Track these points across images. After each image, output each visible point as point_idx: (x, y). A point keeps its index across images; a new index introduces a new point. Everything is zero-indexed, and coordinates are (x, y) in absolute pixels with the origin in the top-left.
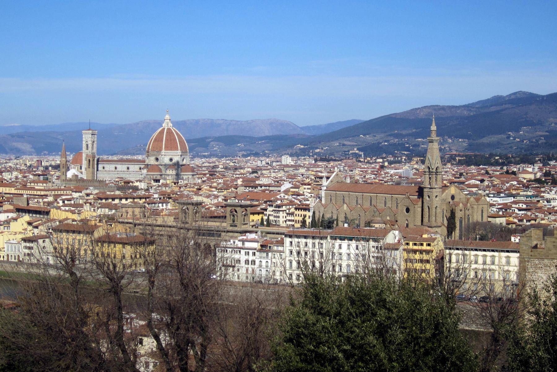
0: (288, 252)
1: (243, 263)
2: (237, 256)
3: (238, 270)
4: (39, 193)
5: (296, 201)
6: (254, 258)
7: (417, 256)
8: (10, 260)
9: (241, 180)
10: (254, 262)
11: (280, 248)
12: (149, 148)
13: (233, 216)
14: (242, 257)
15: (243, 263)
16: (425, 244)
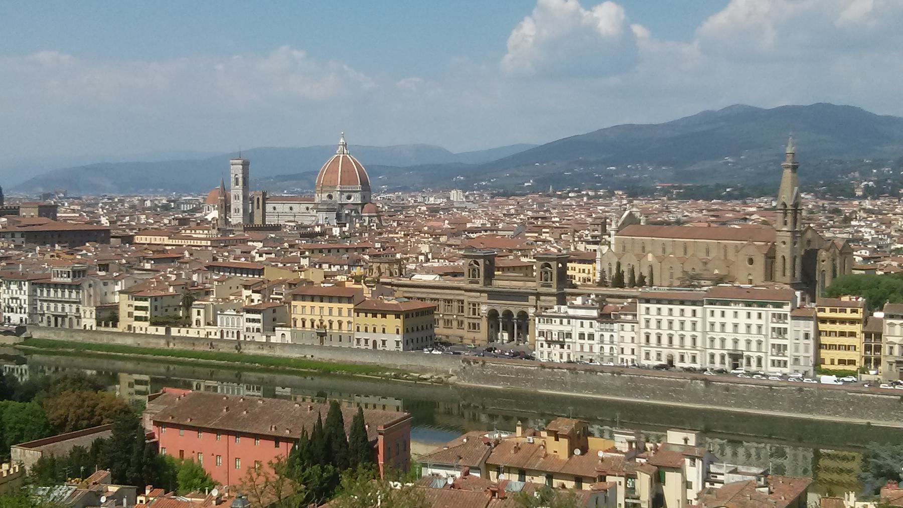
0: (643, 323)
1: (575, 336)
2: (566, 328)
3: (569, 347)
4: (204, 243)
5: (552, 249)
6: (592, 330)
7: (838, 327)
8: (225, 338)
9: (447, 222)
10: (591, 337)
11: (630, 317)
12: (319, 181)
13: (546, 273)
14: (575, 328)
15: (575, 336)
16: (849, 310)
